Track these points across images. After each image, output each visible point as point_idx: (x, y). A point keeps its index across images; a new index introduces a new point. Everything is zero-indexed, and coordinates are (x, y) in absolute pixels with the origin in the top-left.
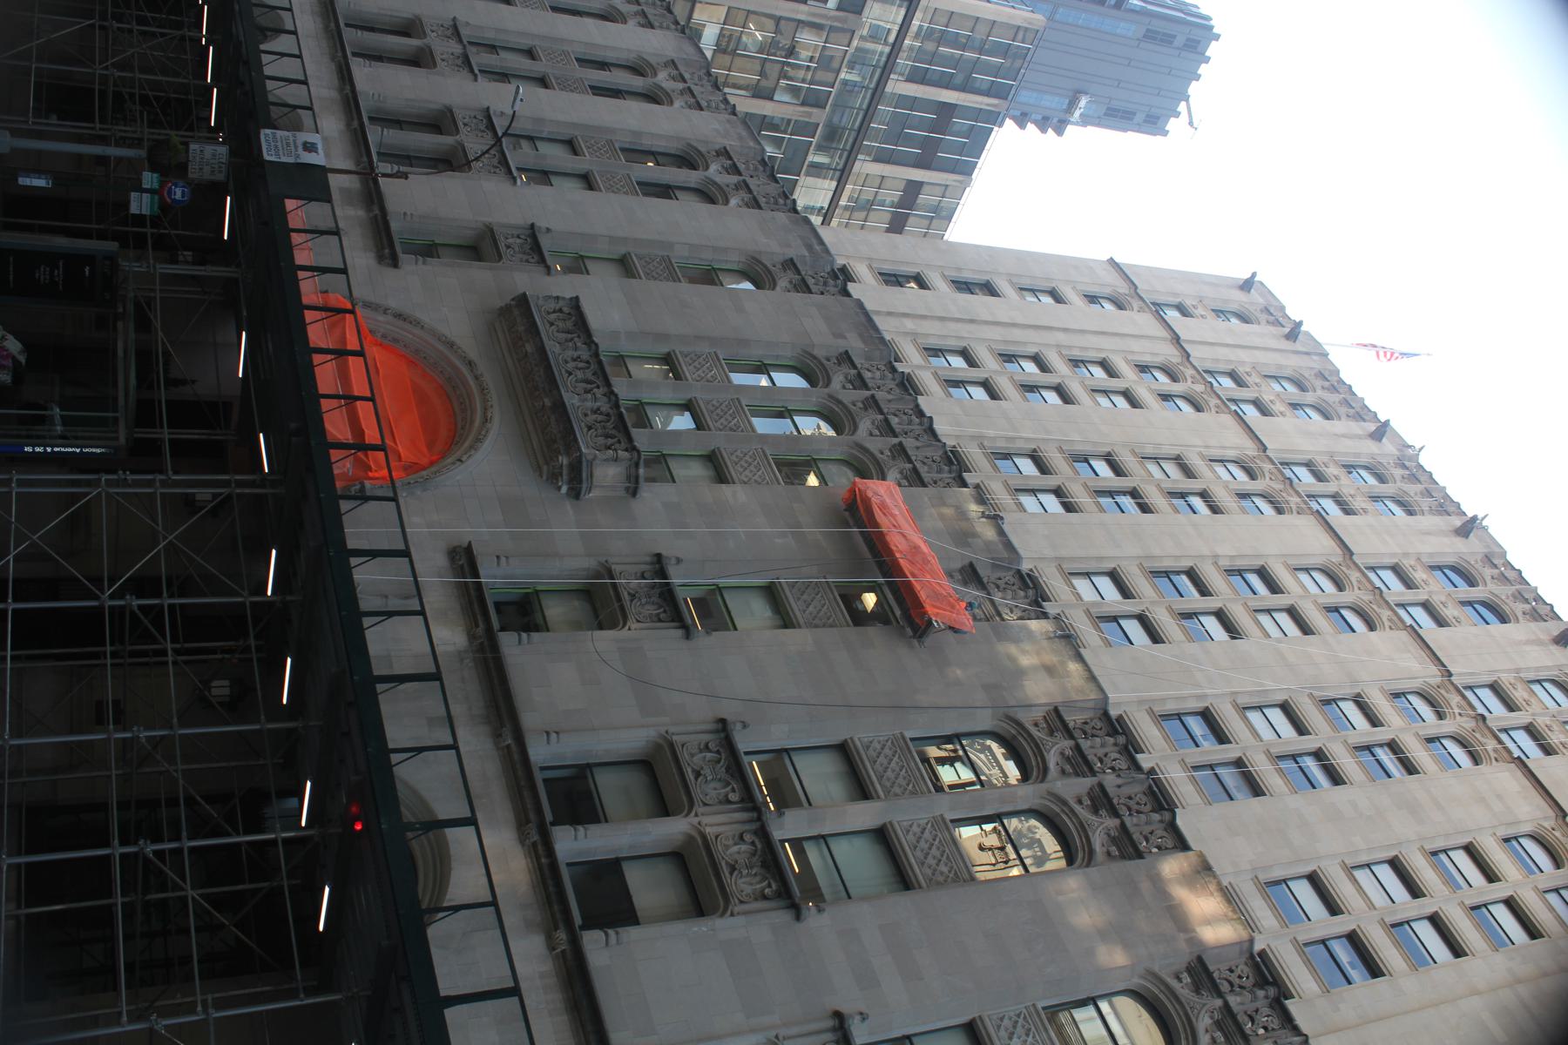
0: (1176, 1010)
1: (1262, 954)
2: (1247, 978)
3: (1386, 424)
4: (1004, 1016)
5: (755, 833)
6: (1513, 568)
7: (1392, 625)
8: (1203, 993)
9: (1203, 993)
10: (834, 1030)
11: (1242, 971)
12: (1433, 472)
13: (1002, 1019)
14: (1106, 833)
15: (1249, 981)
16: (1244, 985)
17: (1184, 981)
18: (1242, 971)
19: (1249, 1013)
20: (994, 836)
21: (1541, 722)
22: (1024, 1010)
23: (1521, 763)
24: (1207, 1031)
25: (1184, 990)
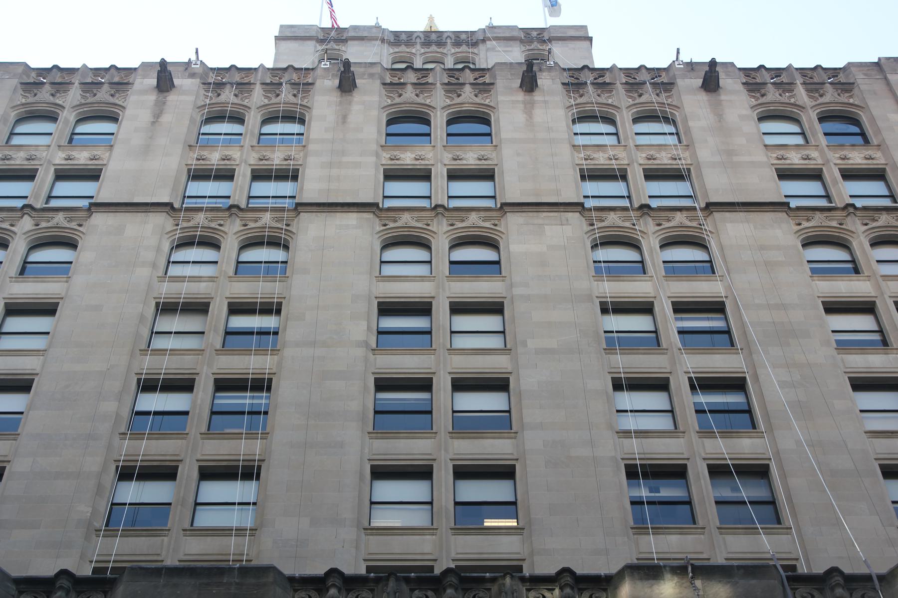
3: (163, 64)
6: (106, 70)
7: (79, 222)
12: (55, 64)
21: (60, 159)
23: (97, 206)
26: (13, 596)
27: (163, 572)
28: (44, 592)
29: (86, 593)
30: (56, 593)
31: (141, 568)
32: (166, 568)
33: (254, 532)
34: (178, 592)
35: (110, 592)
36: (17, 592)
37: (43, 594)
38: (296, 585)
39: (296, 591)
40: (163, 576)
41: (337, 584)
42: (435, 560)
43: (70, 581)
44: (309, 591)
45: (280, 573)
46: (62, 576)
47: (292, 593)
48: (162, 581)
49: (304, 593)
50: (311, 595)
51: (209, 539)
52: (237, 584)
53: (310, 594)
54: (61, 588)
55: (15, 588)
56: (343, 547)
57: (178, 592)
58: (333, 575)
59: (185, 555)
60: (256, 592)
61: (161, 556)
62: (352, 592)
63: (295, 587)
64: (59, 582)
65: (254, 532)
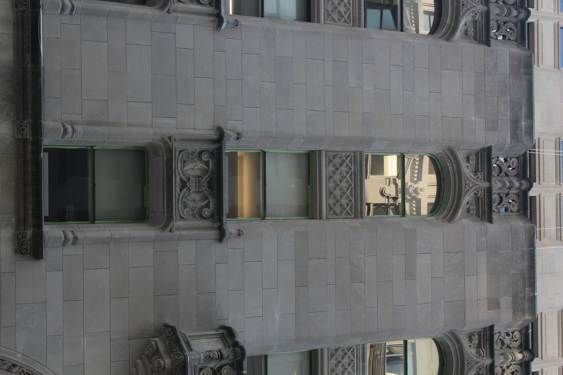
0: (455, 179)
1: (533, 198)
2: (513, 169)
4: (337, 154)
5: (212, 154)
8: (480, 175)
9: (480, 175)
10: (213, 142)
11: (513, 163)
13: (335, 157)
14: (475, 194)
15: (513, 171)
16: (509, 173)
17: (471, 162)
18: (513, 163)
19: (501, 195)
20: (393, 186)
22: (352, 154)
24: (468, 203)
25: (467, 170)
26: (516, 154)
27: (532, 249)
28: (518, 172)
29: (518, 199)
30: (517, 181)
31: (534, 234)
32: (534, 249)
33: (559, 239)
34: (519, 261)
35: (519, 214)
36: (518, 156)
37: (517, 172)
38: (524, 331)
39: (520, 331)
40: (529, 249)
41: (525, 359)
42: (542, 358)
43: (525, 188)
44: (520, 340)
45: (532, 360)
46: (528, 184)
47: (519, 329)
48: (526, 249)
49: (519, 336)
50: (518, 341)
51: (555, 211)
52: (524, 297)
53: (518, 341)
54: (521, 185)
55: (521, 154)
56: (550, 299)
57: (519, 261)
58: (531, 356)
59: (544, 198)
60: (519, 309)
61: (543, 182)
62: (520, 367)
63: (523, 330)
64: (524, 182)
65: (559, 239)
